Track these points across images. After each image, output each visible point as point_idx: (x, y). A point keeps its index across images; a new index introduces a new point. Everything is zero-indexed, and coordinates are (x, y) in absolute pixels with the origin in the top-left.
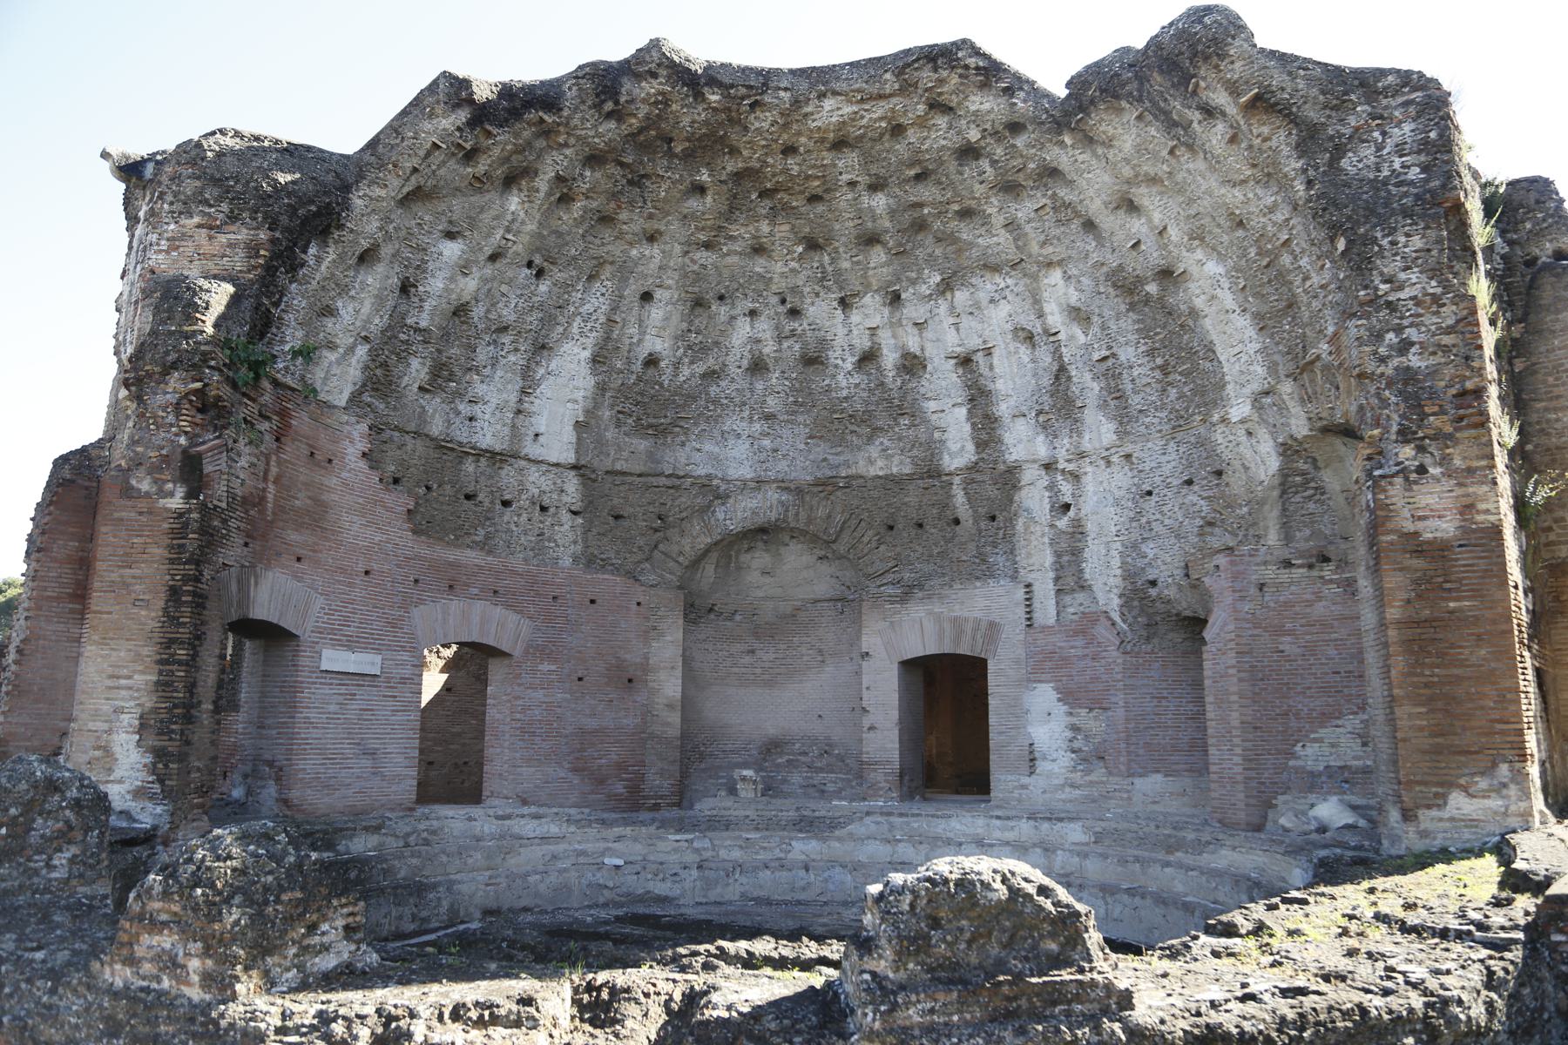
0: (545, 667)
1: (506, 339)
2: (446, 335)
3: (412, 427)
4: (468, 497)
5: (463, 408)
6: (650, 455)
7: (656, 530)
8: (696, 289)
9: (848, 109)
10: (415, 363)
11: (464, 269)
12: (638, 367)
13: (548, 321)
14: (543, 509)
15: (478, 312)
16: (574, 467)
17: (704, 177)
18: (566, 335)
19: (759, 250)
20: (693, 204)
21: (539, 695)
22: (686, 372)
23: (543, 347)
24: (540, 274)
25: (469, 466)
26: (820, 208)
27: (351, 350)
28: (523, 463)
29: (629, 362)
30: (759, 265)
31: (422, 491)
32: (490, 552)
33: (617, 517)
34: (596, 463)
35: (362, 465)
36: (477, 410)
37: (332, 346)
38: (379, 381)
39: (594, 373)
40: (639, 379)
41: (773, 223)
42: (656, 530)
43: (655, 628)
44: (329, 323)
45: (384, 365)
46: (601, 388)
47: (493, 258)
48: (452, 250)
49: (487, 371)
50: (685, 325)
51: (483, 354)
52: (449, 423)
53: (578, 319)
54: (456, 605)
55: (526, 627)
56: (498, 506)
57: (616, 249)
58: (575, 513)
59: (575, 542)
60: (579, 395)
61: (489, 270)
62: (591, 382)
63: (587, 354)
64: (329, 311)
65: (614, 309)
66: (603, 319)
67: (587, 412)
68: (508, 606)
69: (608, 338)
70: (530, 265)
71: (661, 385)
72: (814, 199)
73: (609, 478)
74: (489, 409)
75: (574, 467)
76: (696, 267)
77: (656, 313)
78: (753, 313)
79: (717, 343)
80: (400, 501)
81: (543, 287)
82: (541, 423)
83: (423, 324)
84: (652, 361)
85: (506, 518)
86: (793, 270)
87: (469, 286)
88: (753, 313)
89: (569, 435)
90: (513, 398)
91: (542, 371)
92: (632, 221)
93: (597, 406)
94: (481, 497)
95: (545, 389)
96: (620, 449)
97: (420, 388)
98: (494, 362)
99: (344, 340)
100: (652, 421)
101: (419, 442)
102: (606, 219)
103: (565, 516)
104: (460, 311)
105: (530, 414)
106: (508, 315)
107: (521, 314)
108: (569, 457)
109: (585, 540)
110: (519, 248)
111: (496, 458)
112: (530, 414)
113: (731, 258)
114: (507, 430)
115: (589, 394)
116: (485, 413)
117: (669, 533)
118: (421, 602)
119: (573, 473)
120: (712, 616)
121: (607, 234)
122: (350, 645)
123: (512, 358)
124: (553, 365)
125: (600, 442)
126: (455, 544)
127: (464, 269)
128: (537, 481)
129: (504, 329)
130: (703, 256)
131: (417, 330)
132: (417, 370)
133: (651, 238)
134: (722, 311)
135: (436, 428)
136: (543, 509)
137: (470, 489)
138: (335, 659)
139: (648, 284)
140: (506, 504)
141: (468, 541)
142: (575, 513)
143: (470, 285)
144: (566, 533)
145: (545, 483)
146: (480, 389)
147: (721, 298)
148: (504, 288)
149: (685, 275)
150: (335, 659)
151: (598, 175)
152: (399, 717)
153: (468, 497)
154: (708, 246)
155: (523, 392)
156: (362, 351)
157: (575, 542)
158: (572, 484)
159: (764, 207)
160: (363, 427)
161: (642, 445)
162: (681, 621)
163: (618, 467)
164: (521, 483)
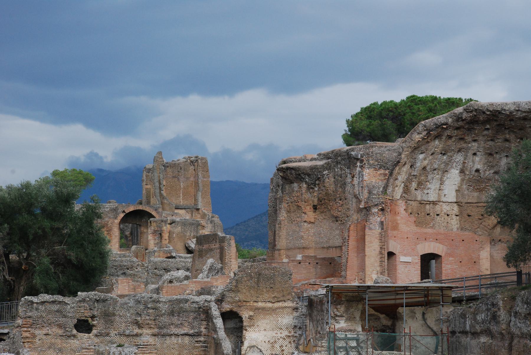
0: (451, 259)
1: (435, 172)
2: (420, 175)
3: (413, 199)
4: (428, 215)
5: (426, 191)
6: (478, 197)
7: (481, 219)
8: (489, 152)
9: (524, 114)
10: (413, 183)
11: (425, 159)
12: (473, 173)
13: (447, 164)
14: (448, 215)
15: (428, 168)
16: (456, 203)
17: (488, 126)
18: (452, 167)
19: (507, 140)
20: (486, 132)
21: (449, 266)
22: (488, 173)
23: (446, 171)
24: (444, 154)
25: (428, 207)
26: (523, 131)
27: (400, 185)
28: (442, 203)
29: (470, 172)
30: (507, 145)
31: (417, 215)
32: (434, 229)
33: (469, 216)
34: (462, 201)
35: (404, 212)
36: (429, 191)
37: (397, 186)
38: (406, 190)
39: (460, 176)
40: (474, 176)
41: (509, 134)
42: (481, 219)
43: (481, 247)
44: (396, 181)
45: (407, 186)
46: (463, 180)
47: (432, 154)
48: (421, 156)
49: (430, 181)
50: (486, 161)
51: (430, 177)
52: (422, 196)
53: (455, 163)
54: (427, 244)
55: (445, 248)
56: (436, 216)
57: (464, 145)
58: (457, 216)
59: (457, 224)
60: (456, 183)
61: (431, 157)
62: (459, 179)
63: (458, 171)
64: (397, 179)
65: (465, 159)
66: (462, 162)
67: (459, 187)
68: (440, 243)
69: (464, 167)
70: (441, 153)
71: (480, 177)
72: (520, 129)
73: (466, 204)
74: (432, 190)
75: (456, 203)
76: (488, 146)
77: (477, 159)
78: (507, 156)
79: (497, 165)
80: (413, 219)
81: (445, 157)
82: (446, 192)
83: (415, 174)
84: (477, 171)
85: (438, 219)
86: (517, 146)
87: (426, 162)
88: (507, 156)
89: (454, 194)
90: (438, 186)
91: (445, 178)
92: (469, 138)
93: (461, 185)
94: (431, 214)
95: (446, 183)
96: (469, 196)
97: (415, 189)
98: (433, 178)
99: (399, 184)
100: (479, 187)
101: (415, 202)
102: (462, 139)
103: (454, 217)
104: (424, 168)
105: (443, 190)
106: (436, 166)
107: (439, 165)
108: (455, 201)
109: (460, 223)
110: (439, 151)
111: (434, 203)
112: (443, 190)
113: (499, 142)
114: (437, 195)
115: (459, 182)
116: (431, 192)
117: (485, 219)
118: (419, 243)
119: (455, 204)
120: (500, 243)
121: (462, 142)
122: (405, 255)
123: (437, 176)
124: (448, 176)
125: (463, 195)
126: (426, 228)
127: (425, 159)
128: (446, 208)
129: (435, 170)
130: (490, 143)
131: (414, 176)
132: (414, 185)
133: (475, 141)
134: (498, 156)
135: (419, 198)
136: (448, 215)
137: (428, 212)
138: (403, 259)
139: (473, 152)
140: (438, 215)
141: (429, 226)
142: (457, 216)
143: (426, 162)
144: (455, 222)
145: (448, 208)
146: (429, 186)
147: (497, 153)
148: (435, 160)
149: (485, 148)
150: (403, 259)
151: (458, 131)
152: (416, 272)
153: (428, 215)
154: (491, 140)
155: (441, 184)
156: (403, 185)
157: (457, 224)
158: (456, 208)
159: (507, 131)
160: (404, 203)
161: (476, 194)
162: (489, 245)
163: (469, 201)
164: (442, 209)
